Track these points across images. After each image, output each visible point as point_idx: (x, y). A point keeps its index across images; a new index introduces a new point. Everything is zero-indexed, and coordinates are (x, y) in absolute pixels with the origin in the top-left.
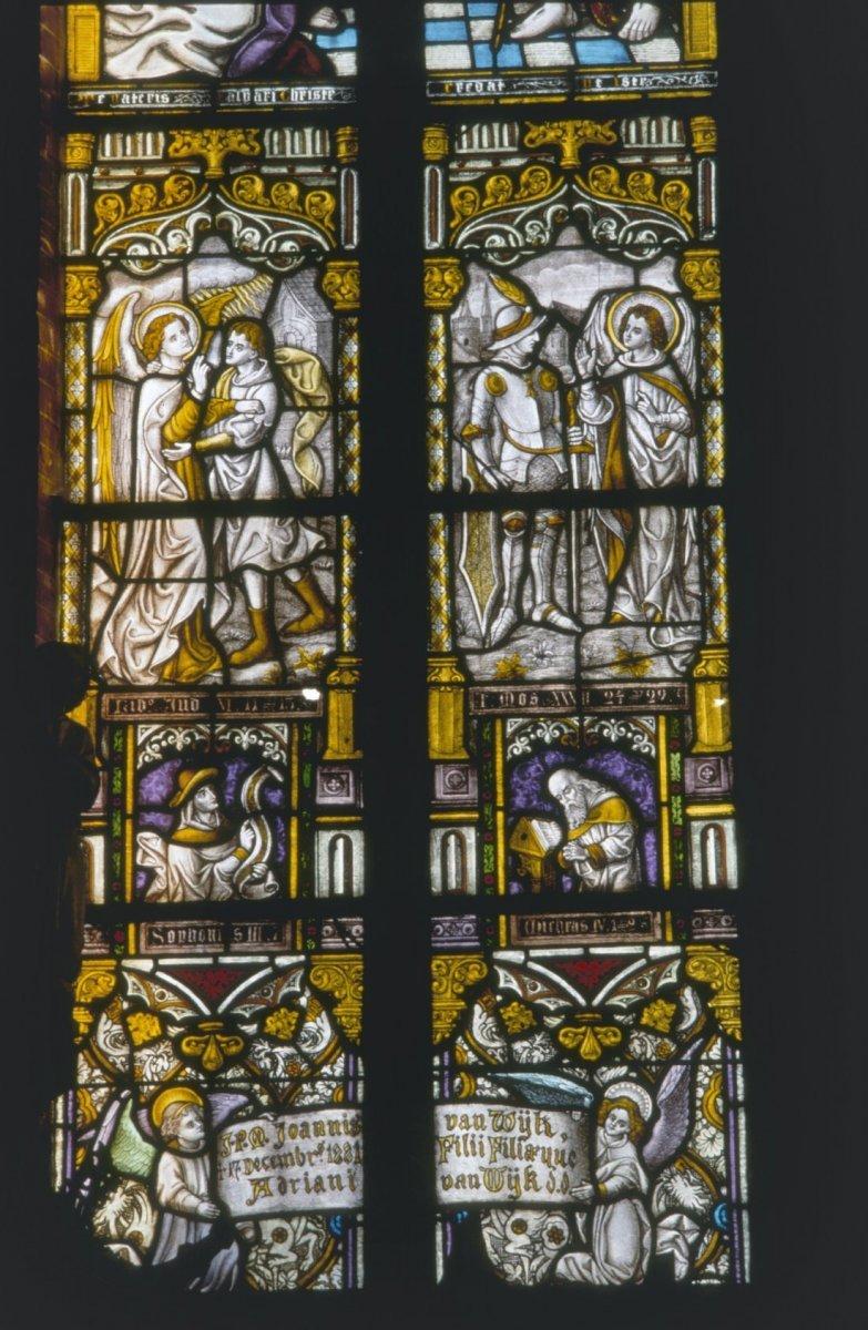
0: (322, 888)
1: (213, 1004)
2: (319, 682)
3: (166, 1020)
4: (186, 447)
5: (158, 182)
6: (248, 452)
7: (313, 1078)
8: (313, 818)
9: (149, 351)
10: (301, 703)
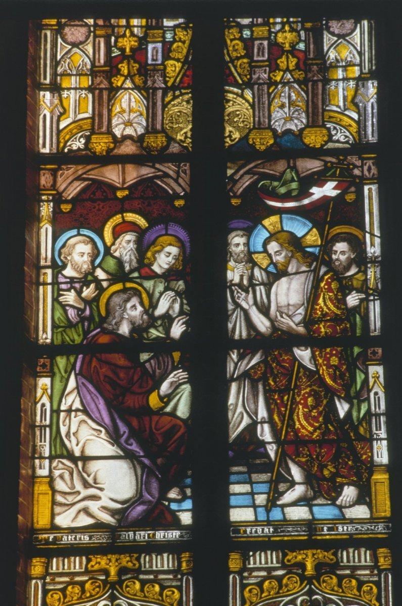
5: (82, 584)
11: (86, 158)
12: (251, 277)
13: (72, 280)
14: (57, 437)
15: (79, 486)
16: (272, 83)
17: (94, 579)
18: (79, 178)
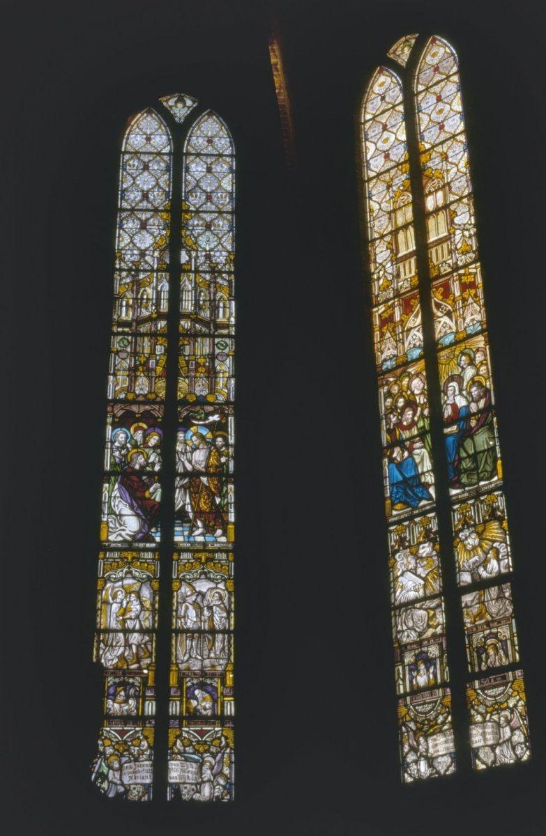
0: (146, 713)
1: (122, 737)
2: (147, 668)
3: (112, 741)
4: (121, 618)
5: (118, 562)
6: (134, 619)
7: (143, 754)
8: (144, 698)
9: (115, 597)
10: (143, 673)
11: (125, 401)
12: (186, 449)
13: (118, 447)
14: (110, 507)
15: (118, 526)
16: (195, 377)
17: (122, 560)
18: (122, 409)
